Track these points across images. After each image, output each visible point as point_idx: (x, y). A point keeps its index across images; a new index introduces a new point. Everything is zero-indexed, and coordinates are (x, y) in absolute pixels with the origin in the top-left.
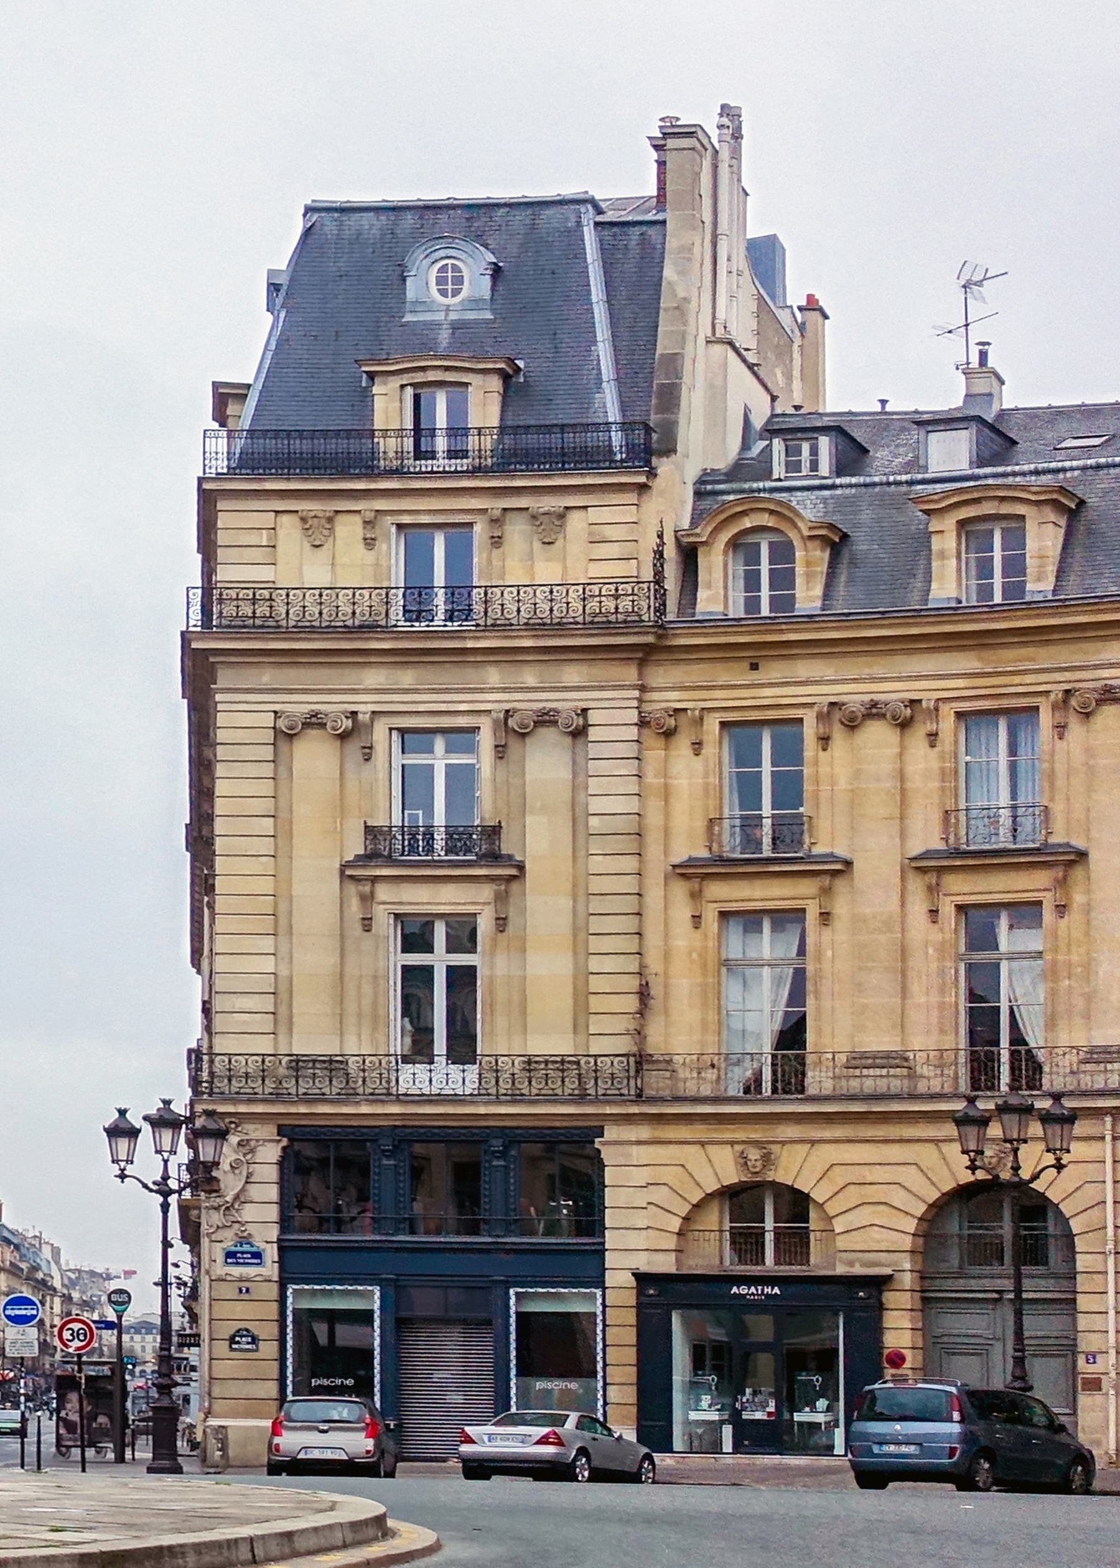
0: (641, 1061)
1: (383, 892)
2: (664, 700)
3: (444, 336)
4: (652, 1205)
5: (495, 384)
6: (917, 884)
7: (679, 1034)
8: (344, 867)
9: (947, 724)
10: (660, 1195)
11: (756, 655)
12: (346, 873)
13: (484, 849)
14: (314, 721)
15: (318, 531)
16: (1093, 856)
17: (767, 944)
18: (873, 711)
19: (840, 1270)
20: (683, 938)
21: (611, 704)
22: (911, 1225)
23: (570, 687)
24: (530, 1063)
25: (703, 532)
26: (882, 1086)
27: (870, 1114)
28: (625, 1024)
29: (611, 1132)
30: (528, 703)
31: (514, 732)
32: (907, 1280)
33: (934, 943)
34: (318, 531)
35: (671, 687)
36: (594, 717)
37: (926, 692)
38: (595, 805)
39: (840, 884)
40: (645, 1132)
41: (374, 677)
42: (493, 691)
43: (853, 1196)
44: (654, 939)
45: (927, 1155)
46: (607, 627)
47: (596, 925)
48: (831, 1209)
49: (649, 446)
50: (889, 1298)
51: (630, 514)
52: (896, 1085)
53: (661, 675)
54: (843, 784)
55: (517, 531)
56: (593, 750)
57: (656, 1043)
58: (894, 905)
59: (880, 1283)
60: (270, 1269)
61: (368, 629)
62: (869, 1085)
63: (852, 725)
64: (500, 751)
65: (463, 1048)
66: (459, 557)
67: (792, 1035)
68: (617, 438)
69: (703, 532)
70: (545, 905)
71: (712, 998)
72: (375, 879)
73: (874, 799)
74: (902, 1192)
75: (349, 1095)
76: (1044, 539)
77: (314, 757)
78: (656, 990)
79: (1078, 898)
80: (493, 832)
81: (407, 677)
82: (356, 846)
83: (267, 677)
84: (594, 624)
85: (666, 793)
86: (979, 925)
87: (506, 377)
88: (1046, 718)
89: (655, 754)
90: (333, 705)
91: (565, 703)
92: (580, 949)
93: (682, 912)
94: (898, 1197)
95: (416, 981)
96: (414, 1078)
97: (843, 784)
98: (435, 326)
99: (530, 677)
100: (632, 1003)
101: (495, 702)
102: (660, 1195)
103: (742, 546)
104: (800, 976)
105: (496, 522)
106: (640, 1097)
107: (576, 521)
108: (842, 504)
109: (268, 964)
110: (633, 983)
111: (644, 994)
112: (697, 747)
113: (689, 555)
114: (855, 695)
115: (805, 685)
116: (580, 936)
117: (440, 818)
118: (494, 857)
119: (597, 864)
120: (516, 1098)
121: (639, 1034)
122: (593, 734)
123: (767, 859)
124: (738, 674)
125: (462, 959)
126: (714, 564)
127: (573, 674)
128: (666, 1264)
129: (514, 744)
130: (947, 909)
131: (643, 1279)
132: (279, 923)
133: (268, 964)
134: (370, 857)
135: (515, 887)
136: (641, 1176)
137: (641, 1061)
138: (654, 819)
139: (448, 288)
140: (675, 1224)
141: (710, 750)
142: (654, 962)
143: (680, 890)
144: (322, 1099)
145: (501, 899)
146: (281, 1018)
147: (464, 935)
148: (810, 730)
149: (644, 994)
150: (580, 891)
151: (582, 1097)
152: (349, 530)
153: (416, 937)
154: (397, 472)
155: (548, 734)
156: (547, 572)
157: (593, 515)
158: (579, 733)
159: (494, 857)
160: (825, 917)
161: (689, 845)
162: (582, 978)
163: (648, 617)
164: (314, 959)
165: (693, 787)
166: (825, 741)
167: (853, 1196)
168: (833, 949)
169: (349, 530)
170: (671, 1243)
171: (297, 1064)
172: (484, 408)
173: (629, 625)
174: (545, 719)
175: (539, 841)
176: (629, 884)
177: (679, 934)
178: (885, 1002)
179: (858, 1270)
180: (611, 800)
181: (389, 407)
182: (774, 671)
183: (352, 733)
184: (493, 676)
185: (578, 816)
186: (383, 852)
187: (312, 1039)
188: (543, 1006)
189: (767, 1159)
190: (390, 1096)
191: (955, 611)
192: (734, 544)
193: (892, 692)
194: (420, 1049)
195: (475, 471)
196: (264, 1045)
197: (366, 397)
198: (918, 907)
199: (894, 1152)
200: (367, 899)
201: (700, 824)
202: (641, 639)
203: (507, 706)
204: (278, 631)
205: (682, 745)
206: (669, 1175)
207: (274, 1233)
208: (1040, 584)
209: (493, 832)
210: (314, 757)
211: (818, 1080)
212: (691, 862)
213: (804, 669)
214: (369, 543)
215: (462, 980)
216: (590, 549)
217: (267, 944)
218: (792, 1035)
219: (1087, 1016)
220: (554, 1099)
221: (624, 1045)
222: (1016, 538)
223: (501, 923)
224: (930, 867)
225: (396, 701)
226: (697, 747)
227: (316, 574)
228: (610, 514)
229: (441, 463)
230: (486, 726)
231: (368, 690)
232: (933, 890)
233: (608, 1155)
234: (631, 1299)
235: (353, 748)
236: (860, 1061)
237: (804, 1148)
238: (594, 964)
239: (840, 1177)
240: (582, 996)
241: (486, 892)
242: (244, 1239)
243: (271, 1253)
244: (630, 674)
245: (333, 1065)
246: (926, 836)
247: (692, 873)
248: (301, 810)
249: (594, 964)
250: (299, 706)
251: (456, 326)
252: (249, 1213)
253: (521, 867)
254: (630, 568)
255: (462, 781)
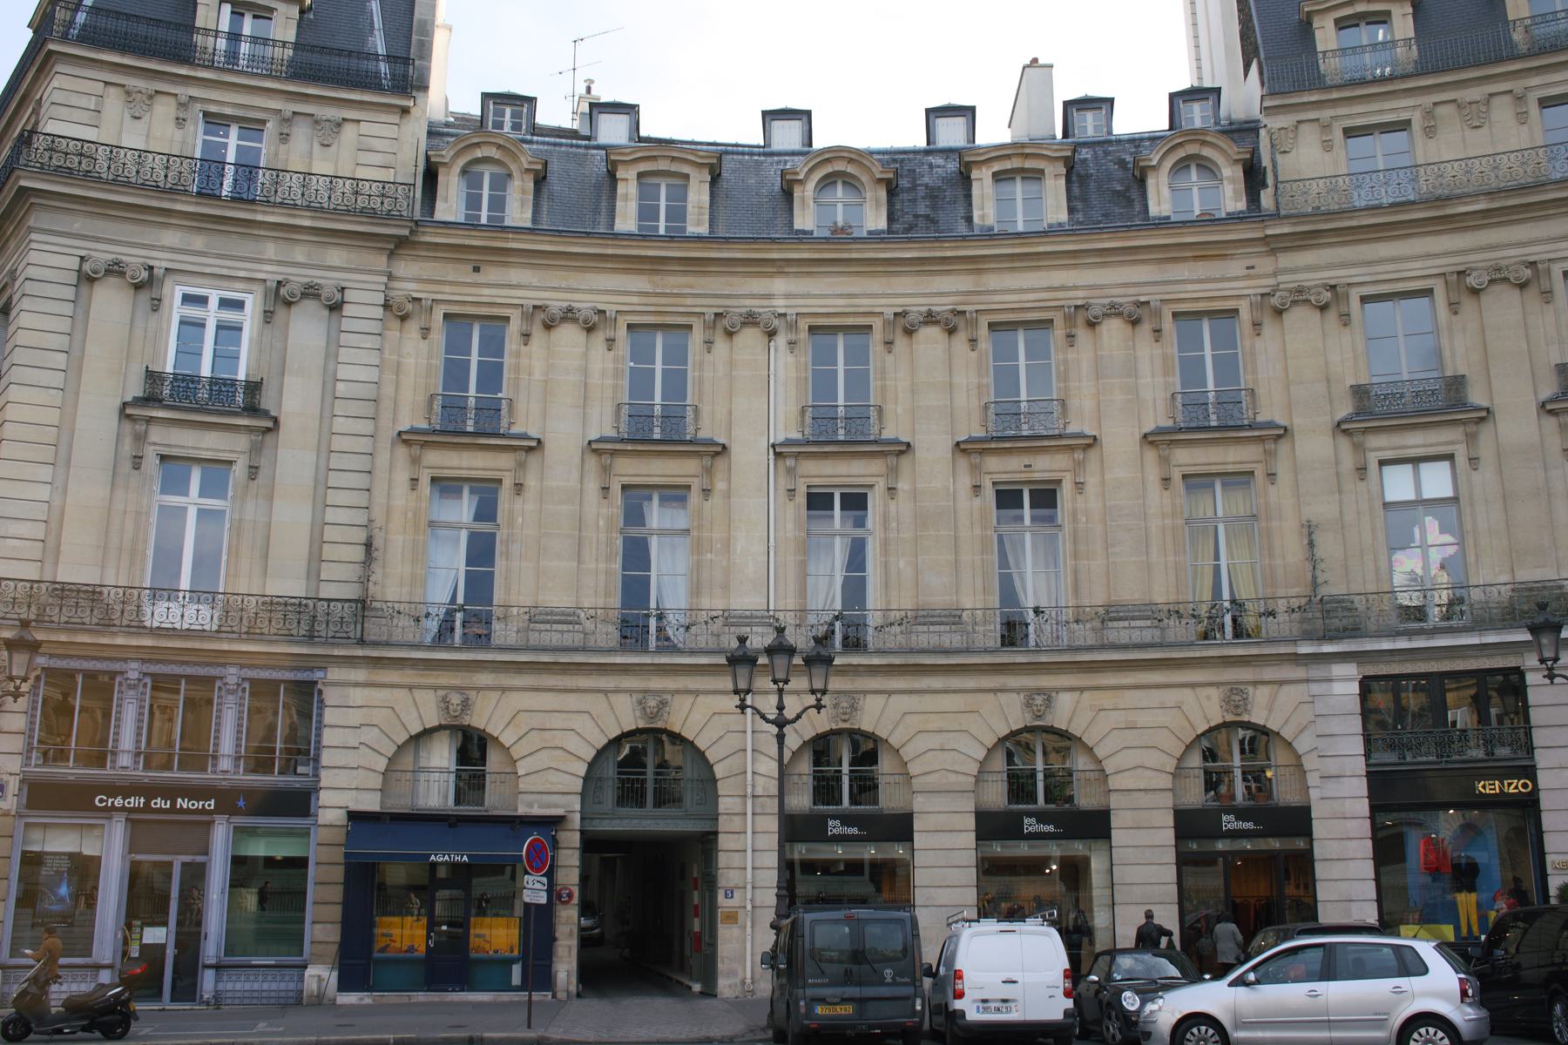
0: (362, 606)
1: (156, 434)
8: (125, 404)
12: (124, 412)
14: (115, 270)
22: (582, 769)
23: (334, 265)
30: (298, 278)
31: (280, 300)
36: (349, 295)
41: (171, 238)
43: (535, 740)
46: (371, 214)
48: (516, 753)
56: (346, 324)
64: (268, 316)
70: (293, 458)
72: (150, 420)
74: (577, 738)
81: (198, 242)
82: (136, 389)
90: (134, 258)
91: (328, 281)
92: (321, 505)
94: (573, 743)
99: (299, 254)
100: (358, 554)
101: (271, 273)
106: (361, 642)
110: (361, 536)
111: (368, 545)
116: (321, 487)
118: (252, 409)
121: (364, 581)
122: (348, 310)
127: (336, 256)
129: (281, 312)
134: (150, 399)
135: (269, 438)
137: (362, 606)
145: (256, 450)
150: (325, 450)
151: (311, 637)
155: (310, 305)
158: (336, 308)
159: (252, 409)
167: (535, 740)
174: (311, 292)
175: (295, 401)
180: (356, 370)
183: (147, 285)
184: (271, 250)
185: (330, 380)
189: (466, 705)
199: (572, 701)
200: (140, 438)
203: (280, 278)
210: (110, 301)
216: (367, 151)
221: (351, 592)
223: (253, 472)
231: (163, 245)
235: (144, 297)
237: (495, 695)
238: (331, 515)
240: (317, 543)
241: (242, 442)
249: (331, 515)
253: (276, 420)
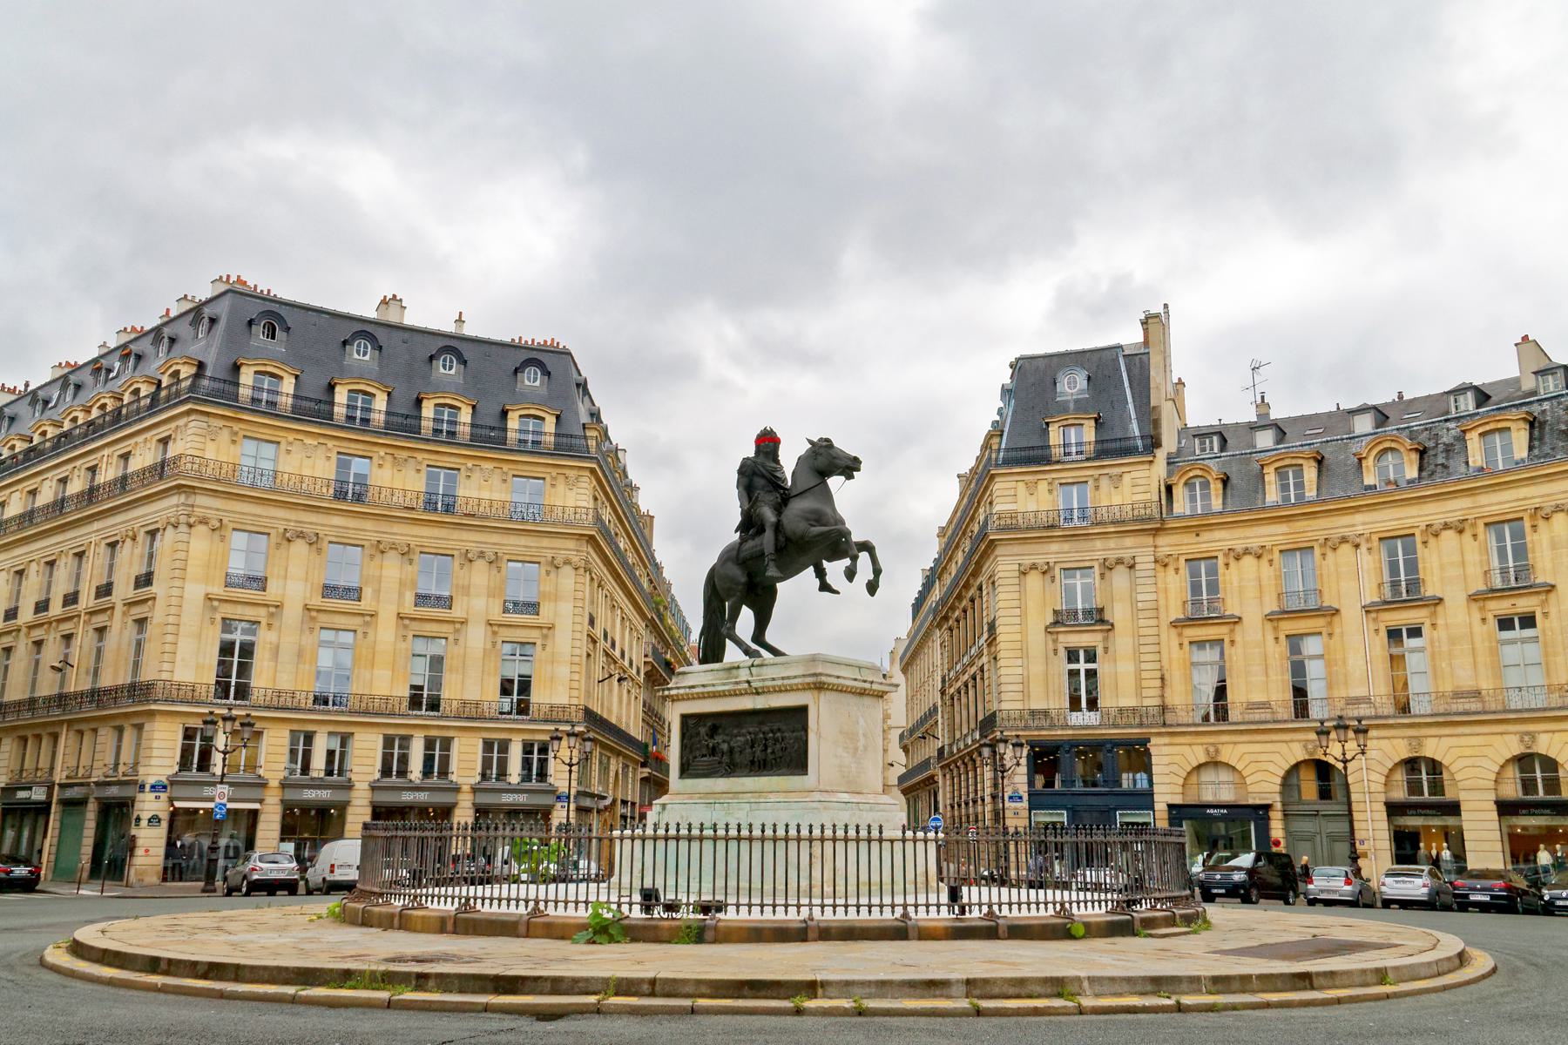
0: (1164, 709)
1: (1061, 638)
2: (1164, 551)
3: (1072, 406)
4: (1170, 775)
5: (1092, 423)
6: (1269, 626)
7: (1176, 697)
9: (1276, 555)
10: (1174, 768)
11: (1197, 530)
13: (1098, 617)
14: (1034, 567)
15: (1031, 488)
16: (1343, 611)
17: (1210, 655)
18: (1247, 552)
19: (1251, 802)
20: (1176, 653)
21: (1141, 550)
22: (1279, 781)
23: (1128, 546)
24: (1121, 710)
25: (1174, 479)
26: (1263, 717)
27: (1256, 730)
28: (1157, 692)
29: (1154, 741)
30: (1112, 556)
31: (1107, 567)
32: (1279, 806)
33: (1278, 653)
34: (1031, 488)
35: (1167, 544)
36: (1138, 560)
37: (1267, 542)
38: (1140, 597)
39: (1237, 627)
40: (1166, 740)
41: (1055, 547)
42: (1101, 549)
43: (1253, 768)
44: (1165, 655)
45: (1283, 748)
46: (1142, 520)
47: (1143, 649)
49: (1153, 443)
50: (1272, 814)
51: (1146, 473)
52: (1269, 717)
53: (1163, 540)
54: (1235, 584)
55: (1105, 483)
56: (1138, 574)
57: (1169, 701)
58: (1259, 636)
59: (1267, 807)
60: (1025, 804)
61: (1052, 527)
62: (1257, 717)
63: (1238, 558)
64: (1102, 575)
65: (1093, 704)
66: (1082, 497)
67: (1221, 692)
68: (1139, 443)
69: (1174, 479)
70: (1123, 640)
71: (1188, 679)
73: (1248, 589)
75: (1052, 727)
76: (1310, 473)
77: (1034, 580)
78: (1167, 677)
79: (1337, 631)
80: (1101, 611)
81: (1066, 546)
82: (1050, 619)
83: (1016, 549)
84: (1136, 520)
85: (1166, 590)
86: (1294, 641)
87: (1096, 420)
88: (1317, 551)
89: (1161, 575)
90: (1040, 560)
91: (1126, 555)
93: (1175, 643)
94: (1272, 768)
95: (1073, 674)
96: (1077, 718)
97: (1235, 584)
98: (1067, 402)
99: (1112, 543)
100: (1158, 683)
101: (1100, 555)
102: (1174, 768)
103: (1189, 484)
104: (1222, 669)
105: (1096, 480)
107: (1126, 478)
108: (1229, 462)
109: (1019, 670)
110: (1158, 674)
111: (1162, 679)
112: (1177, 570)
113: (1169, 489)
114: (1239, 546)
115: (1217, 541)
116: (1137, 654)
117: (1080, 606)
118: (1102, 621)
119: (1142, 623)
120: (1115, 726)
123: (1204, 617)
124: (1191, 538)
125: (1091, 666)
126: (1179, 492)
127: (1129, 541)
128: (1178, 800)
129: (1107, 573)
130: (1282, 638)
131: (1171, 807)
132: (1023, 652)
133: (1019, 670)
134: (1056, 623)
136: (1166, 760)
137: (1164, 709)
138: (1162, 602)
139: (1072, 386)
140: (1181, 781)
141: (1182, 571)
142: (1165, 663)
143: (1174, 632)
144: (1042, 728)
145: (1106, 639)
146: (1025, 694)
147: (1091, 657)
148: (1221, 561)
149: (1162, 679)
151: (1141, 725)
152: (1043, 486)
153: (1072, 656)
154: (1058, 462)
155: (1121, 568)
156: (1117, 500)
157: (1134, 475)
158: (1132, 567)
159: (1102, 621)
160: (1232, 642)
161: (1176, 613)
162: (1139, 671)
163: (1157, 516)
164: (1037, 667)
165: (1174, 589)
166: (1227, 565)
167: (1253, 768)
168: (1235, 655)
169: (1043, 486)
170: (1180, 790)
171: (1033, 713)
172: (1089, 433)
173: (1151, 519)
174: (1120, 561)
175: (1119, 614)
176: (1154, 631)
177: (1174, 650)
178: (1259, 682)
179: (1258, 802)
181: (1055, 436)
182: (1205, 536)
184: (1098, 544)
185: (1134, 602)
186: (1061, 620)
187: (1037, 704)
188: (1123, 687)
189: (1217, 751)
190: (1066, 727)
191: (1277, 507)
192: (1186, 484)
193: (1254, 544)
194: (1075, 704)
195: (1088, 459)
196: (1019, 706)
197: (1045, 432)
198: (1270, 638)
199: (1269, 747)
200: (1055, 641)
201: (1179, 603)
202: (1154, 525)
204: (1017, 529)
205: (1171, 570)
206: (1177, 759)
207: (1026, 788)
208: (1311, 493)
209: (1101, 611)
210: (1034, 580)
211: (1234, 715)
212: (1178, 620)
213: (1218, 534)
214: (1050, 491)
215: (1091, 674)
216: (1134, 486)
217: (1019, 662)
218: (1221, 692)
219: (1346, 683)
220: (1131, 726)
221: (1157, 702)
222: (1299, 474)
223: (1106, 649)
224: (1272, 618)
225: (1062, 557)
226: (1177, 570)
227: (1032, 507)
228: (1140, 473)
229: (1074, 457)
230: (1096, 565)
231: (1054, 552)
232: (1276, 629)
233: (1153, 751)
234: (1166, 815)
235: (1048, 577)
236: (1252, 706)
238: (1144, 666)
239: (1247, 758)
241: (1099, 636)
242: (1015, 791)
243: (1026, 797)
244: (1149, 540)
245: (1046, 713)
246: (1271, 605)
247: (1175, 624)
248: (1030, 604)
249: (1144, 666)
250: (1028, 561)
251: (1077, 401)
252: (1017, 779)
254: (1148, 496)
255: (1087, 590)
